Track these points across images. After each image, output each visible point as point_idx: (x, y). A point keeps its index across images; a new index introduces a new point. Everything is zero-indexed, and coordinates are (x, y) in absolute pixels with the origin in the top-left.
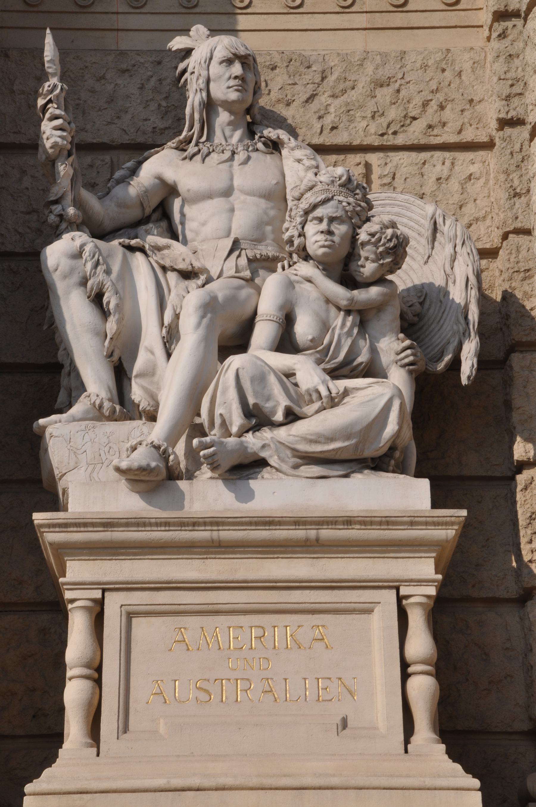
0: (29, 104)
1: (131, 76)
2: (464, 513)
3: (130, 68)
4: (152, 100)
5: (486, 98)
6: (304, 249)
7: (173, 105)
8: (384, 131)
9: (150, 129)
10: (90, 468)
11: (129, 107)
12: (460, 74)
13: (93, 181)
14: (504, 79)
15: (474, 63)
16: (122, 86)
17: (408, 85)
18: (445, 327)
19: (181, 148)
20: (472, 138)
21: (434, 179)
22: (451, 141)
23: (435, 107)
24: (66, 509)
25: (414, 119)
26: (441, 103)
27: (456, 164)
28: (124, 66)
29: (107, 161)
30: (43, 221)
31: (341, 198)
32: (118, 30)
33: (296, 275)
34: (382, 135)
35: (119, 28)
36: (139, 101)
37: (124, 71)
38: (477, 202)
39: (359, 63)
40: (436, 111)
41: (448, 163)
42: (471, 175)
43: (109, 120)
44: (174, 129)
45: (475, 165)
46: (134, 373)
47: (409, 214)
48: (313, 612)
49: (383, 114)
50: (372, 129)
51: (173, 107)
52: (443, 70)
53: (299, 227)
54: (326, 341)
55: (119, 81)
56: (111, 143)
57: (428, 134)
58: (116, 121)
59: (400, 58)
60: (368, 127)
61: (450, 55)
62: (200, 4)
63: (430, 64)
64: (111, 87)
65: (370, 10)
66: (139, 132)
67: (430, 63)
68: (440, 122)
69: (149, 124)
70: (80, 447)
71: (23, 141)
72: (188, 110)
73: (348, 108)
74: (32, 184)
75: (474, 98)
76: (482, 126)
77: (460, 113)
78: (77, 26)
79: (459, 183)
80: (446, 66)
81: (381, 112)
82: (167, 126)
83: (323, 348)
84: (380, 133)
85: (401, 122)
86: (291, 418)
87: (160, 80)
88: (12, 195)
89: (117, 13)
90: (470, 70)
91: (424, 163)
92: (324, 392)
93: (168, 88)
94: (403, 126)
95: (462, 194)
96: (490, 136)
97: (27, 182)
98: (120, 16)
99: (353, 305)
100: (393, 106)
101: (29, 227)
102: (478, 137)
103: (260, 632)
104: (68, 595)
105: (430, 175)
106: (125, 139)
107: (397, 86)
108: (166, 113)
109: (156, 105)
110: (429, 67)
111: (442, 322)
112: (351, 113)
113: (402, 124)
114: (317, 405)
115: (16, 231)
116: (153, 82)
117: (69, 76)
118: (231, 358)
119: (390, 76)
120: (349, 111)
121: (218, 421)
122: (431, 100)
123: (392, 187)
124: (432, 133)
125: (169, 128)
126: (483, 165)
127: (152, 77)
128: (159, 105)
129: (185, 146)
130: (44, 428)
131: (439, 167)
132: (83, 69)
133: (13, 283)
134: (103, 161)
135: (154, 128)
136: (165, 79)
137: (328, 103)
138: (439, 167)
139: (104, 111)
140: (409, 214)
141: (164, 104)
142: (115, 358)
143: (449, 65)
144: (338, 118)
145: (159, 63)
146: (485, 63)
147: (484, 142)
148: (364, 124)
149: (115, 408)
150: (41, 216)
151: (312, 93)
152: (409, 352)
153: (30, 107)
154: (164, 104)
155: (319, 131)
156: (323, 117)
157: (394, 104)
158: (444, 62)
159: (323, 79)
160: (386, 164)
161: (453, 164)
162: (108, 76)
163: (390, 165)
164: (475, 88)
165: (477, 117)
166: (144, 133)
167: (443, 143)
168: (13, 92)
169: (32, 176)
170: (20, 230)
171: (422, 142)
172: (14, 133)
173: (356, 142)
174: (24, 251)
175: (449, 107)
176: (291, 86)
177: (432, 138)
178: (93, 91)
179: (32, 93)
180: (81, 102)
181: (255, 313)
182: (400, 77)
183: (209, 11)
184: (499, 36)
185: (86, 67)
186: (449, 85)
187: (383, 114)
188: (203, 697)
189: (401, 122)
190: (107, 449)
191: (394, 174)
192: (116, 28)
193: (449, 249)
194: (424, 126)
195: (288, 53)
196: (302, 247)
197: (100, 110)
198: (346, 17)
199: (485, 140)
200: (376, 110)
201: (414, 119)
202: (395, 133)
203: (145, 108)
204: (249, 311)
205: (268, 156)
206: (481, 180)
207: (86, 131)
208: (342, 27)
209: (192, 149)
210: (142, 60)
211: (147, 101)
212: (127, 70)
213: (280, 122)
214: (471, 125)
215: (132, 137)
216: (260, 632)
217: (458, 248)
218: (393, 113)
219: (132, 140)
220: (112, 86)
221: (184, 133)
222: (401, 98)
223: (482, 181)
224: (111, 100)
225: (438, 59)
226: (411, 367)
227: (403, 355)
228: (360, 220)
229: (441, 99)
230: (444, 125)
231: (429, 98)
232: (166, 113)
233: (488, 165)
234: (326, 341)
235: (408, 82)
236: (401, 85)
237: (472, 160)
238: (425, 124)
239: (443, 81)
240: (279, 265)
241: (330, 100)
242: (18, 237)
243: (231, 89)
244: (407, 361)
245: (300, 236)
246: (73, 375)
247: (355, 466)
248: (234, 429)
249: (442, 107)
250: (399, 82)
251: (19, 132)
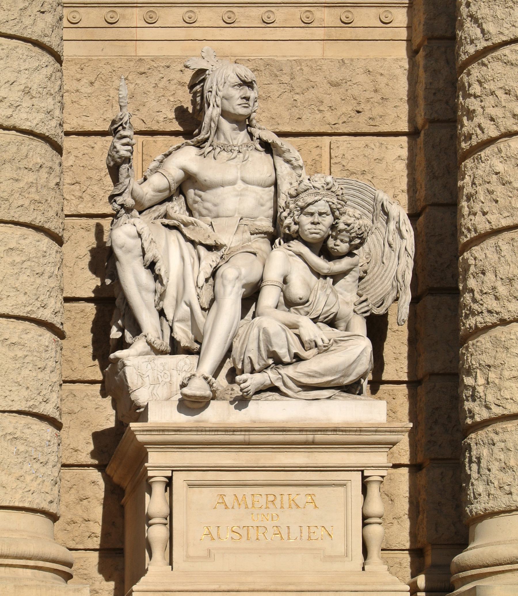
3: (146, 71)
9: (162, 119)
16: (140, 85)
18: (386, 282)
28: (142, 70)
36: (153, 97)
47: (361, 196)
66: (153, 122)
87: (169, 80)
101: (73, 195)
111: (384, 278)
117: (101, 78)
128: (168, 100)
132: (111, 72)
136: (172, 80)
180: (110, 98)
210: (155, 65)
219: (149, 128)
220: (133, 85)
244: (363, 310)
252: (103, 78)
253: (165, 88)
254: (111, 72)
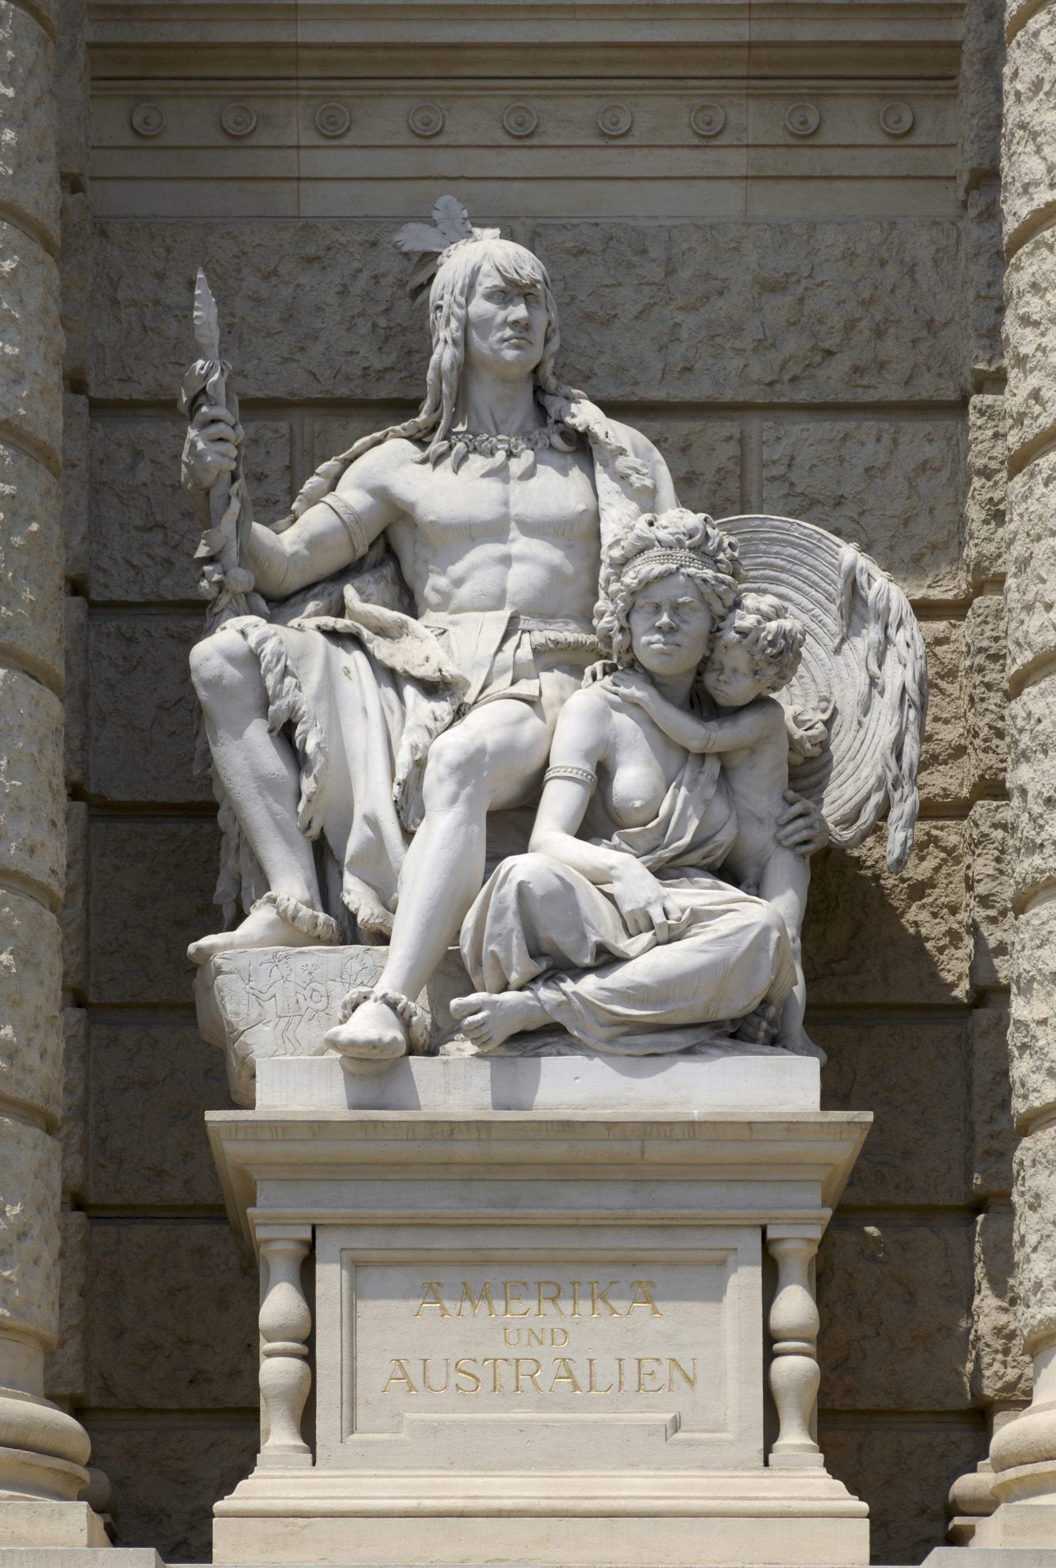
0: (144, 326)
1: (324, 268)
2: (869, 1116)
3: (323, 253)
4: (361, 315)
5: (957, 318)
6: (630, 649)
7: (399, 325)
8: (775, 378)
9: (359, 372)
10: (283, 1023)
11: (321, 330)
12: (911, 272)
13: (259, 470)
14: (985, 297)
15: (937, 251)
16: (308, 288)
17: (820, 289)
19: (420, 441)
20: (931, 394)
21: (860, 470)
22: (894, 399)
23: (867, 333)
24: (251, 1106)
25: (829, 353)
26: (878, 325)
27: (900, 441)
28: (311, 250)
29: (282, 431)
30: (173, 544)
31: (692, 570)
32: (299, 179)
33: (616, 694)
34: (771, 384)
35: (303, 175)
36: (338, 318)
37: (311, 260)
38: (937, 513)
39: (732, 245)
40: (869, 341)
41: (886, 440)
42: (926, 462)
43: (286, 355)
44: (400, 371)
45: (935, 444)
46: (347, 859)
47: (810, 560)
48: (634, 1263)
49: (774, 345)
50: (756, 371)
51: (399, 329)
52: (883, 263)
53: (622, 616)
54: (663, 810)
55: (303, 280)
56: (289, 398)
57: (853, 383)
58: (298, 356)
59: (805, 237)
60: (748, 369)
61: (895, 233)
62: (446, 129)
63: (859, 251)
64: (287, 291)
65: (755, 143)
66: (339, 378)
67: (861, 247)
68: (874, 361)
69: (357, 362)
70: (264, 989)
71: (136, 396)
72: (430, 375)
73: (712, 333)
74: (152, 474)
75: (937, 318)
76: (948, 369)
77: (910, 345)
78: (226, 174)
79: (905, 477)
80: (888, 255)
81: (770, 341)
82: (389, 365)
83: (659, 824)
84: (769, 379)
85: (805, 359)
86: (604, 958)
87: (375, 277)
88: (119, 497)
89: (298, 147)
90: (929, 264)
91: (844, 439)
92: (658, 917)
93: (389, 292)
94: (808, 366)
95: (908, 498)
96: (961, 390)
97: (144, 472)
98: (303, 153)
99: (709, 746)
100: (792, 328)
101: (149, 555)
102: (940, 392)
105: (854, 461)
106: (315, 392)
107: (800, 289)
108: (387, 339)
109: (369, 325)
110: (858, 256)
112: (719, 340)
113: (807, 363)
114: (646, 937)
115: (128, 562)
116: (361, 284)
117: (214, 270)
118: (509, 862)
119: (788, 271)
120: (713, 337)
121: (486, 961)
122: (860, 319)
123: (787, 484)
124: (859, 382)
125: (393, 368)
126: (948, 444)
127: (360, 271)
128: (375, 325)
129: (425, 436)
130: (205, 954)
131: (870, 446)
132: (238, 257)
133: (125, 659)
134: (276, 431)
135: (365, 369)
136: (384, 275)
137: (676, 320)
138: (870, 446)
139: (276, 337)
140: (810, 560)
141: (382, 322)
142: (314, 831)
143: (894, 253)
144: (693, 351)
145: (374, 244)
146: (958, 251)
147: (950, 401)
148: (738, 362)
149: (317, 917)
150: (170, 535)
151: (647, 301)
152: (801, 822)
153: (145, 331)
154: (382, 322)
155: (659, 375)
156: (667, 348)
157: (794, 324)
158: (885, 247)
159: (670, 273)
160: (778, 439)
161: (895, 441)
162: (283, 270)
163: (785, 441)
164: (939, 297)
165: (940, 353)
166: (348, 379)
167: (879, 402)
168: (115, 302)
169: (152, 461)
170: (135, 561)
171: (845, 397)
172: (120, 380)
173: (728, 396)
174: (141, 600)
175: (892, 331)
176: (607, 290)
177: (860, 390)
178: (257, 300)
179: (150, 304)
180: (236, 320)
181: (547, 764)
182: (805, 275)
183: (463, 141)
184: (980, 215)
185: (244, 253)
186: (892, 291)
187: (774, 345)
189: (805, 359)
190: (307, 993)
191: (792, 458)
192: (296, 175)
194: (846, 369)
195: (604, 227)
196: (626, 646)
197: (269, 335)
198: (710, 155)
199: (952, 398)
200: (761, 336)
201: (829, 353)
202: (794, 380)
203: (349, 329)
204: (536, 762)
205: (569, 457)
206: (943, 472)
207: (246, 377)
208: (703, 174)
209: (437, 445)
210: (343, 240)
211: (353, 317)
212: (318, 258)
213: (591, 357)
214: (929, 370)
215: (327, 388)
217: (891, 631)
218: (793, 344)
219: (327, 392)
220: (290, 289)
221: (423, 416)
222: (806, 313)
223: (945, 473)
224: (288, 317)
225: (874, 241)
226: (804, 849)
227: (790, 828)
228: (724, 606)
229: (878, 317)
230: (882, 366)
231: (857, 315)
232: (387, 339)
233: (957, 445)
234: (663, 810)
235: (821, 284)
236: (806, 289)
237: (929, 434)
238: (849, 364)
239: (882, 283)
240: (588, 671)
241: (680, 317)
242: (132, 573)
243: (506, 344)
244: (797, 838)
245: (622, 629)
246: (243, 851)
247: (703, 1035)
248: (514, 977)
249: (879, 334)
250: (804, 283)
251: (129, 379)
252: (219, 270)
253: (367, 297)
254: (238, 257)
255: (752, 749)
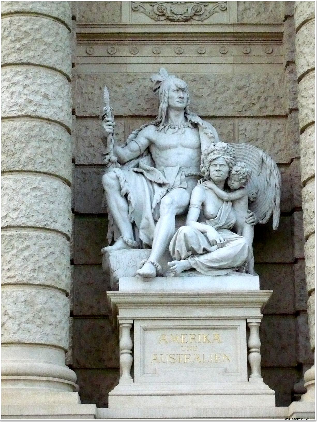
103: (193, 336)
104: (120, 322)
188: (172, 361)
193: (268, 171)
205: (193, 129)
216: (193, 336)
255: (240, 199)
